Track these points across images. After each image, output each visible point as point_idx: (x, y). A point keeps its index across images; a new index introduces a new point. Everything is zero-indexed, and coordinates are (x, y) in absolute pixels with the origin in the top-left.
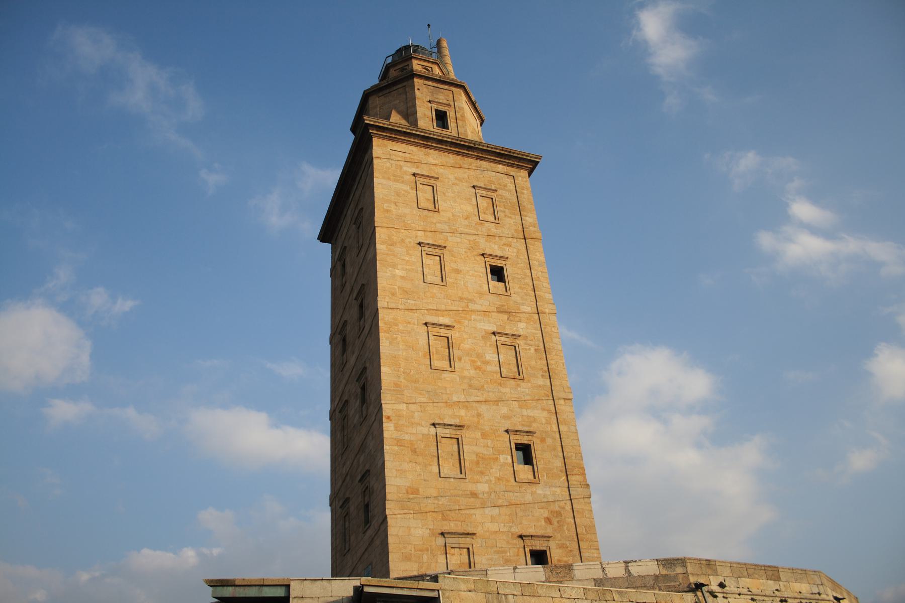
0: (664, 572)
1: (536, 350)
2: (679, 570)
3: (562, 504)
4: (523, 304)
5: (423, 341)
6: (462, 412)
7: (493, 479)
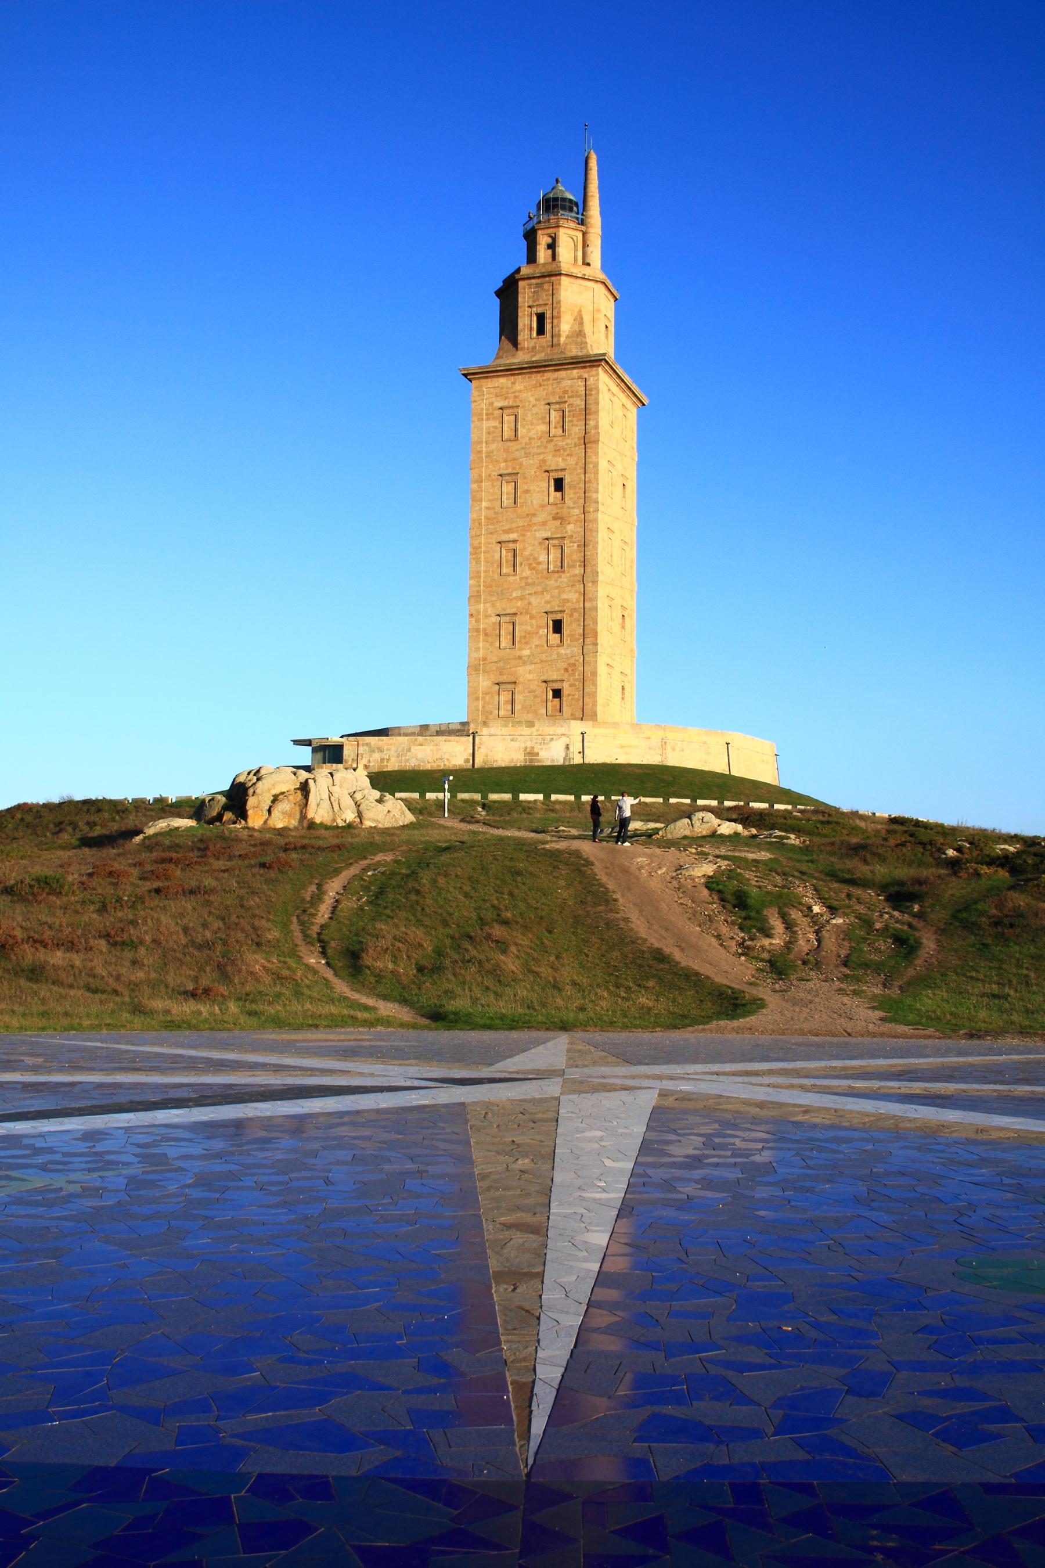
5: (497, 556)
6: (519, 604)
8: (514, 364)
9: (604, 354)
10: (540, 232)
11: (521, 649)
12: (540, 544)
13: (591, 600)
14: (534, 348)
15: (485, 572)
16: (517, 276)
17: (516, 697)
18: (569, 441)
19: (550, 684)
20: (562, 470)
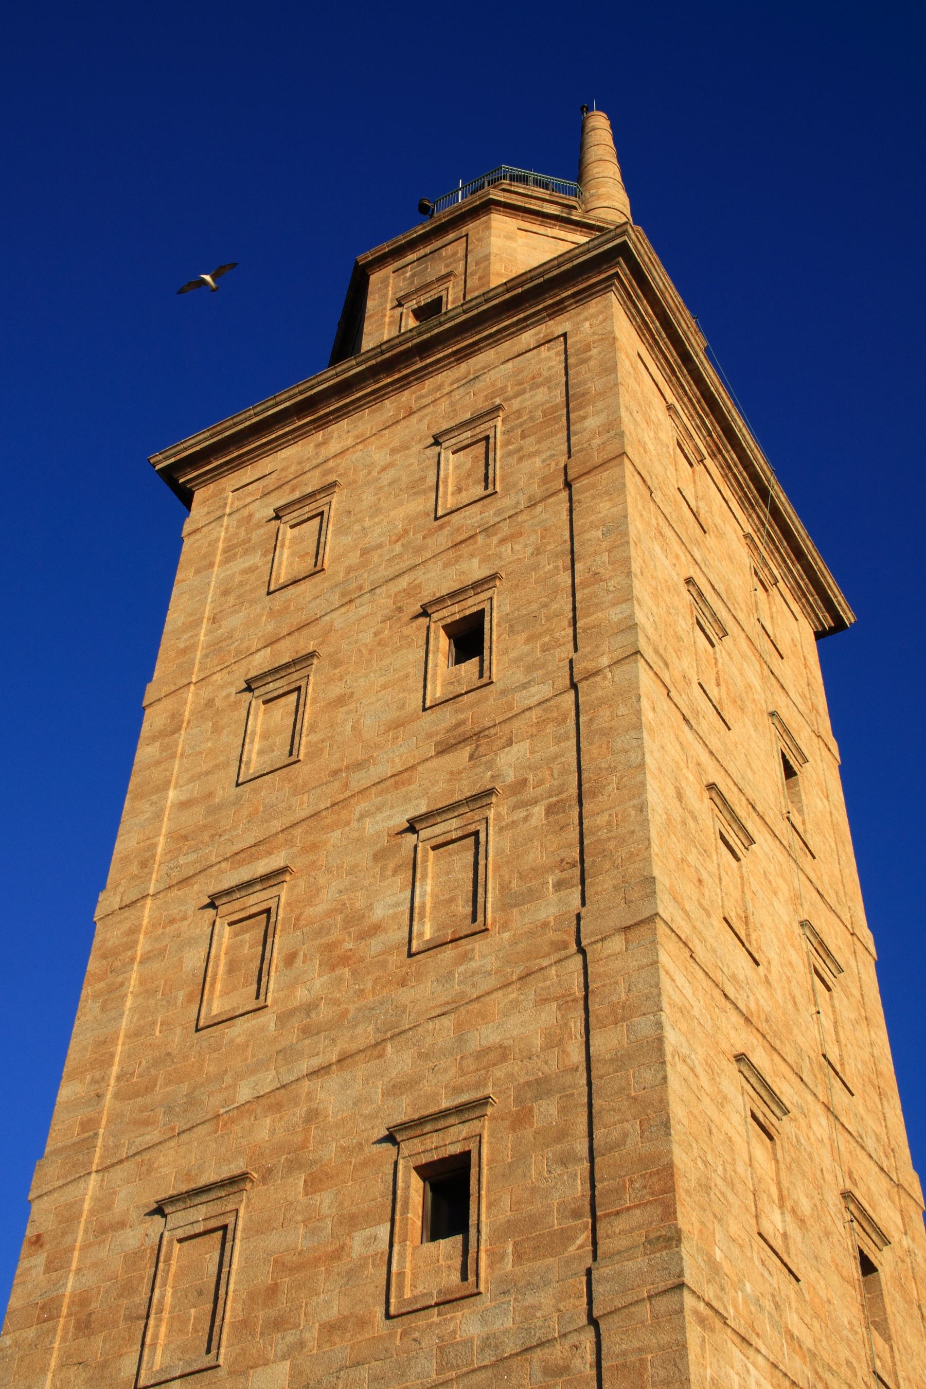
1: (549, 811)
3: (558, 1353)
4: (525, 686)
5: (193, 959)
7: (311, 1335)
13: (622, 1014)
15: (135, 1035)
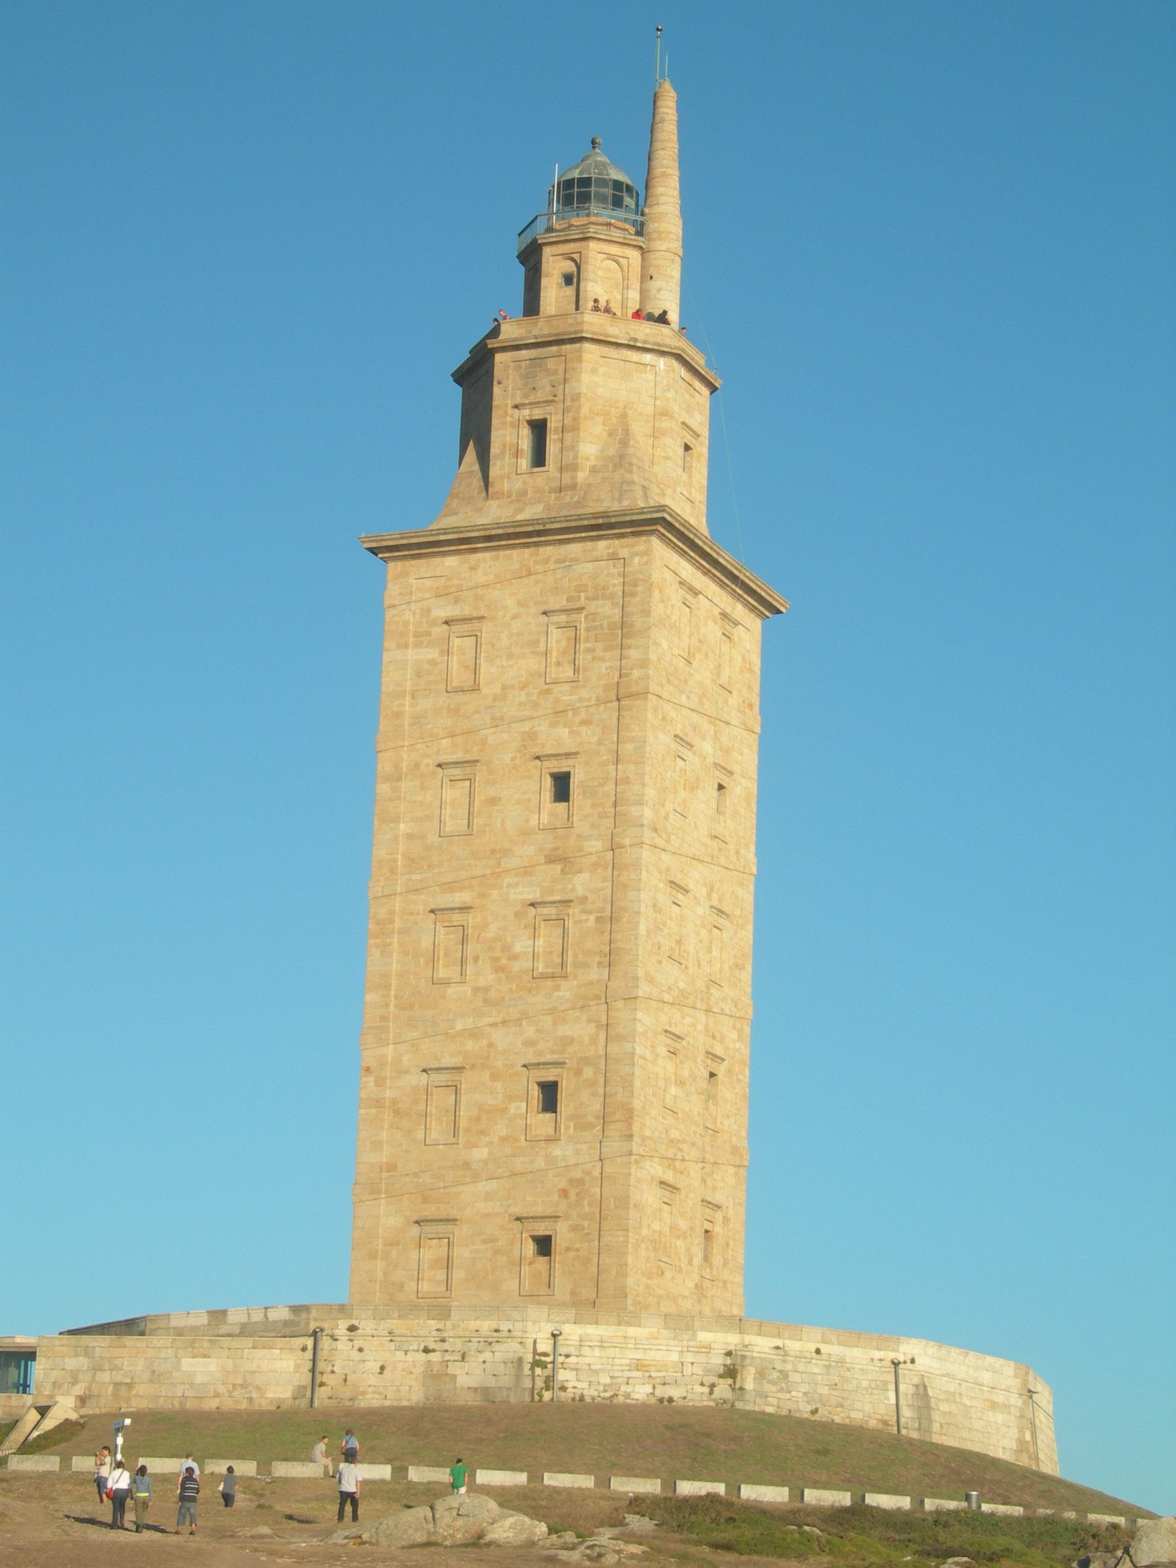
0: (293, 1318)
2: (304, 1315)
5: (426, 942)
6: (470, 1045)
7: (496, 1140)
8: (473, 528)
9: (662, 508)
10: (547, 251)
11: (470, 1146)
12: (518, 915)
13: (620, 1038)
14: (524, 493)
16: (492, 344)
17: (456, 1251)
18: (584, 693)
19: (529, 1225)
20: (568, 755)
